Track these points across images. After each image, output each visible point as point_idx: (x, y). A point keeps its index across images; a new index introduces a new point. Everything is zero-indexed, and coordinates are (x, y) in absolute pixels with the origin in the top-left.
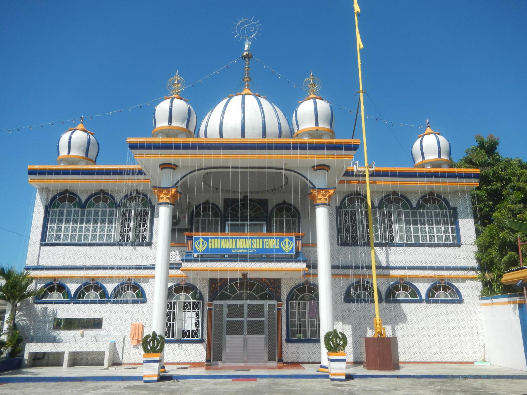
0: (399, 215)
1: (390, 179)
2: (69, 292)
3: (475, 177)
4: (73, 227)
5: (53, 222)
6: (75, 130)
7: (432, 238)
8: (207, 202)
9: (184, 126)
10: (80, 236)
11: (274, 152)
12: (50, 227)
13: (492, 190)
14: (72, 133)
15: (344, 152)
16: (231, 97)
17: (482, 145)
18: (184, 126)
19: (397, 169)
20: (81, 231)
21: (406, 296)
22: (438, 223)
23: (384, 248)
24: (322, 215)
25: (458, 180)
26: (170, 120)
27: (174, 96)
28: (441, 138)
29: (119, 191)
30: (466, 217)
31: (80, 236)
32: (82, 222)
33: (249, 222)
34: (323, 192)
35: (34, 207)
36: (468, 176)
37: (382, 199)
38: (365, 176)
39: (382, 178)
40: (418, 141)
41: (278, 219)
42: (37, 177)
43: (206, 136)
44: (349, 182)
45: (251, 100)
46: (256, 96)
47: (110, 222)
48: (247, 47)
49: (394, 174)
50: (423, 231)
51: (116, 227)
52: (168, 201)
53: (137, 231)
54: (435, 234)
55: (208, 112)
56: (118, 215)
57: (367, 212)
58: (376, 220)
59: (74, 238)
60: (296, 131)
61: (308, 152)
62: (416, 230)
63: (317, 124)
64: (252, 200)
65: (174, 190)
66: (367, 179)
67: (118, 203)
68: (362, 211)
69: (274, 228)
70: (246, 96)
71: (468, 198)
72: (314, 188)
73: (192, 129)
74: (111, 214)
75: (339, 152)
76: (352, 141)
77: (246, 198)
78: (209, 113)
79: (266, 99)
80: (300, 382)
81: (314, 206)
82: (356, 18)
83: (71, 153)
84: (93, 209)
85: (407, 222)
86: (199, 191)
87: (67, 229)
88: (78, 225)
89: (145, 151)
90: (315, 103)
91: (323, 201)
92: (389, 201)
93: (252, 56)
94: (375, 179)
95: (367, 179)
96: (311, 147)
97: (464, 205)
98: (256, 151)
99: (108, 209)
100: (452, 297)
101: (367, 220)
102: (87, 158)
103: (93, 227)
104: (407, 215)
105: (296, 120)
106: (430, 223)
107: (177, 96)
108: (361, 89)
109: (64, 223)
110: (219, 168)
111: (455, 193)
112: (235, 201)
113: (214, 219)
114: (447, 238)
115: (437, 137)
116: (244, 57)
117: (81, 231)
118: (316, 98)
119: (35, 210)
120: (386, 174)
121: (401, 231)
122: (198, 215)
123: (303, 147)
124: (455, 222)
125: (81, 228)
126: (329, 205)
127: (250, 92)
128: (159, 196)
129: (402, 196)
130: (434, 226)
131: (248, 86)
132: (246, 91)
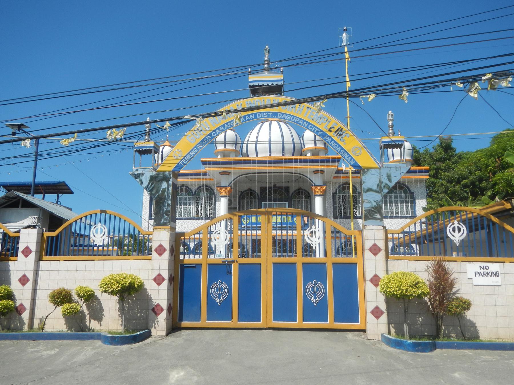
3: (425, 172)
6: (164, 146)
7: (397, 213)
8: (249, 189)
14: (163, 148)
15: (331, 163)
18: (233, 148)
22: (401, 202)
26: (225, 146)
30: (422, 198)
41: (296, 200)
44: (339, 177)
45: (275, 124)
47: (190, 204)
50: (391, 208)
51: (193, 207)
52: (226, 195)
53: (206, 209)
54: (399, 210)
56: (194, 201)
61: (308, 164)
65: (229, 188)
69: (293, 205)
70: (273, 122)
71: (424, 185)
72: (315, 185)
73: (238, 149)
74: (190, 200)
75: (328, 163)
77: (275, 186)
79: (285, 123)
86: (244, 182)
89: (212, 166)
91: (320, 193)
96: (310, 161)
97: (420, 190)
98: (277, 164)
100: (408, 251)
106: (396, 203)
110: (255, 173)
113: (254, 200)
114: (407, 212)
119: (144, 198)
122: (244, 198)
123: (306, 161)
124: (413, 202)
130: (399, 205)
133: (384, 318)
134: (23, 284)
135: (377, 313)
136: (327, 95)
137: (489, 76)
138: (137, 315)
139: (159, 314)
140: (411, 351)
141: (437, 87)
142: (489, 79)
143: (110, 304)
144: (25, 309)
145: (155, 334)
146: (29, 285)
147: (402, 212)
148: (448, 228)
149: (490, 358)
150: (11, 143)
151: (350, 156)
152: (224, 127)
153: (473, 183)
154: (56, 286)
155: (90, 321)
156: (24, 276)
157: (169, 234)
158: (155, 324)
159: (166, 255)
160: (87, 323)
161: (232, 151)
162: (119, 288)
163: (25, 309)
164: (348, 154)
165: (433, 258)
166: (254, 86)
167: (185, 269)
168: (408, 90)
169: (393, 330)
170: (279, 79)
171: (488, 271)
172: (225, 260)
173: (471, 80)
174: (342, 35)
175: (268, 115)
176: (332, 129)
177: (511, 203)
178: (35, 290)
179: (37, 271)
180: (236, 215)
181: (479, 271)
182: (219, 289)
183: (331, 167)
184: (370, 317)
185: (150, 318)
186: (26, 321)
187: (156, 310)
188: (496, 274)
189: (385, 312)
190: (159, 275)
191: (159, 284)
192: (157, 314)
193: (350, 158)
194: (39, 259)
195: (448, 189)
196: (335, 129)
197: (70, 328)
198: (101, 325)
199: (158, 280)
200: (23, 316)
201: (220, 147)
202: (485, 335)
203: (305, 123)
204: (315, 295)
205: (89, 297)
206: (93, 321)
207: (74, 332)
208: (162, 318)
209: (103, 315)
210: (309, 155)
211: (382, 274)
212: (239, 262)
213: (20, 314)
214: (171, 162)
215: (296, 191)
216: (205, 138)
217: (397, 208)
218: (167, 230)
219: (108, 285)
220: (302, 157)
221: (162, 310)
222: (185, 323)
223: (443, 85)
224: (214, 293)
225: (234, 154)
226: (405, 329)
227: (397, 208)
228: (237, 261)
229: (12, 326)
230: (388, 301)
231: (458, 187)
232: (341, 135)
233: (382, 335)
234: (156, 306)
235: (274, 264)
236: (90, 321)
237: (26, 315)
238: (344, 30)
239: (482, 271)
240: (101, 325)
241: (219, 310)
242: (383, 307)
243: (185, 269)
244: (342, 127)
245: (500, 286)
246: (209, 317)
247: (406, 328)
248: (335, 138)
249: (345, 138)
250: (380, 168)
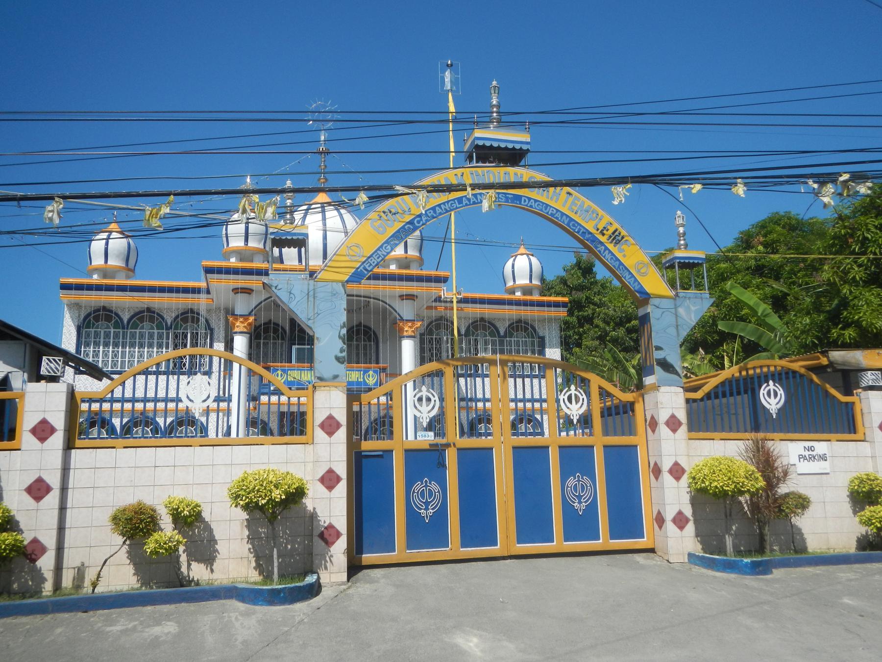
0: (486, 343)
1: (478, 306)
2: (113, 428)
4: (113, 352)
5: (87, 345)
6: (111, 232)
9: (261, 246)
10: (123, 363)
12: (85, 351)
13: (583, 317)
15: (433, 284)
17: (578, 264)
18: (261, 246)
19: (486, 296)
20: (123, 356)
24: (408, 349)
25: (546, 309)
26: (246, 240)
28: (534, 260)
29: (169, 309)
31: (123, 363)
32: (124, 346)
34: (410, 324)
35: (63, 326)
36: (557, 305)
37: (469, 326)
39: (470, 305)
40: (511, 260)
42: (73, 292)
44: (436, 308)
46: (337, 209)
49: (482, 301)
52: (245, 330)
57: (452, 339)
58: (461, 348)
59: (115, 365)
61: (397, 283)
63: (406, 251)
65: (251, 319)
66: (455, 305)
67: (169, 324)
68: (447, 339)
72: (402, 319)
75: (429, 284)
81: (402, 337)
83: (109, 263)
84: (138, 331)
87: (106, 355)
88: (120, 350)
89: (223, 276)
91: (410, 333)
92: (476, 328)
94: (463, 305)
95: (455, 305)
97: (552, 334)
99: (156, 331)
101: (452, 348)
102: (129, 269)
103: (139, 352)
104: (494, 344)
109: (101, 347)
111: (542, 320)
115: (529, 259)
117: (123, 356)
120: (474, 301)
123: (392, 277)
125: (124, 353)
129: (489, 322)
133: (690, 528)
134: (38, 498)
135: (680, 521)
136: (632, 177)
137: (845, 177)
138: (286, 546)
139: (333, 543)
140: (749, 574)
141: (781, 184)
142: (845, 182)
143: (230, 528)
144: (43, 550)
145: (328, 581)
146: (52, 500)
148: (762, 391)
149: (851, 575)
150: (15, 203)
151: (633, 276)
152: (435, 212)
154: (128, 499)
155: (189, 565)
156: (40, 481)
157: (345, 396)
158: (326, 561)
159: (341, 434)
160: (184, 569)
161: (257, 251)
162: (283, 497)
163: (43, 550)
164: (630, 273)
165: (753, 435)
166: (484, 146)
167: (364, 460)
168: (746, 184)
169: (700, 547)
170: (524, 139)
171: (814, 453)
172: (434, 442)
173: (821, 180)
174: (444, 72)
175: (507, 199)
176: (605, 232)
177: (828, 357)
178: (63, 509)
179: (66, 470)
180: (448, 365)
181: (803, 453)
182: (426, 494)
183: (434, 290)
184: (670, 527)
185: (315, 552)
186: (49, 575)
187: (326, 536)
188: (823, 458)
189: (691, 518)
190: (330, 471)
191: (330, 488)
192: (329, 543)
193: (633, 279)
194: (69, 446)
195: (607, 334)
196: (610, 232)
197: (145, 582)
198: (212, 571)
199: (329, 480)
200: (40, 563)
201: (237, 243)
202: (814, 544)
203: (564, 217)
204: (579, 497)
205: (189, 520)
206: (194, 565)
207: (155, 590)
208: (339, 549)
209: (217, 551)
210: (393, 268)
211: (683, 463)
212: (458, 446)
213: (34, 561)
214: (343, 264)
216: (403, 227)
218: (340, 388)
219: (258, 491)
220: (387, 271)
221: (338, 535)
222: (368, 558)
223: (787, 182)
224: (417, 501)
225: (261, 258)
226: (728, 543)
228: (454, 445)
229: (15, 586)
230: (694, 502)
231: (621, 332)
232: (616, 243)
233: (690, 555)
234: (326, 528)
235: (514, 448)
236: (189, 565)
237: (46, 563)
238: (448, 65)
239: (807, 453)
240: (212, 571)
241: (427, 531)
242: (688, 512)
243: (364, 460)
244: (620, 229)
245: (828, 474)
246: (412, 542)
247: (729, 541)
248: (610, 246)
249: (624, 247)
250: (675, 299)
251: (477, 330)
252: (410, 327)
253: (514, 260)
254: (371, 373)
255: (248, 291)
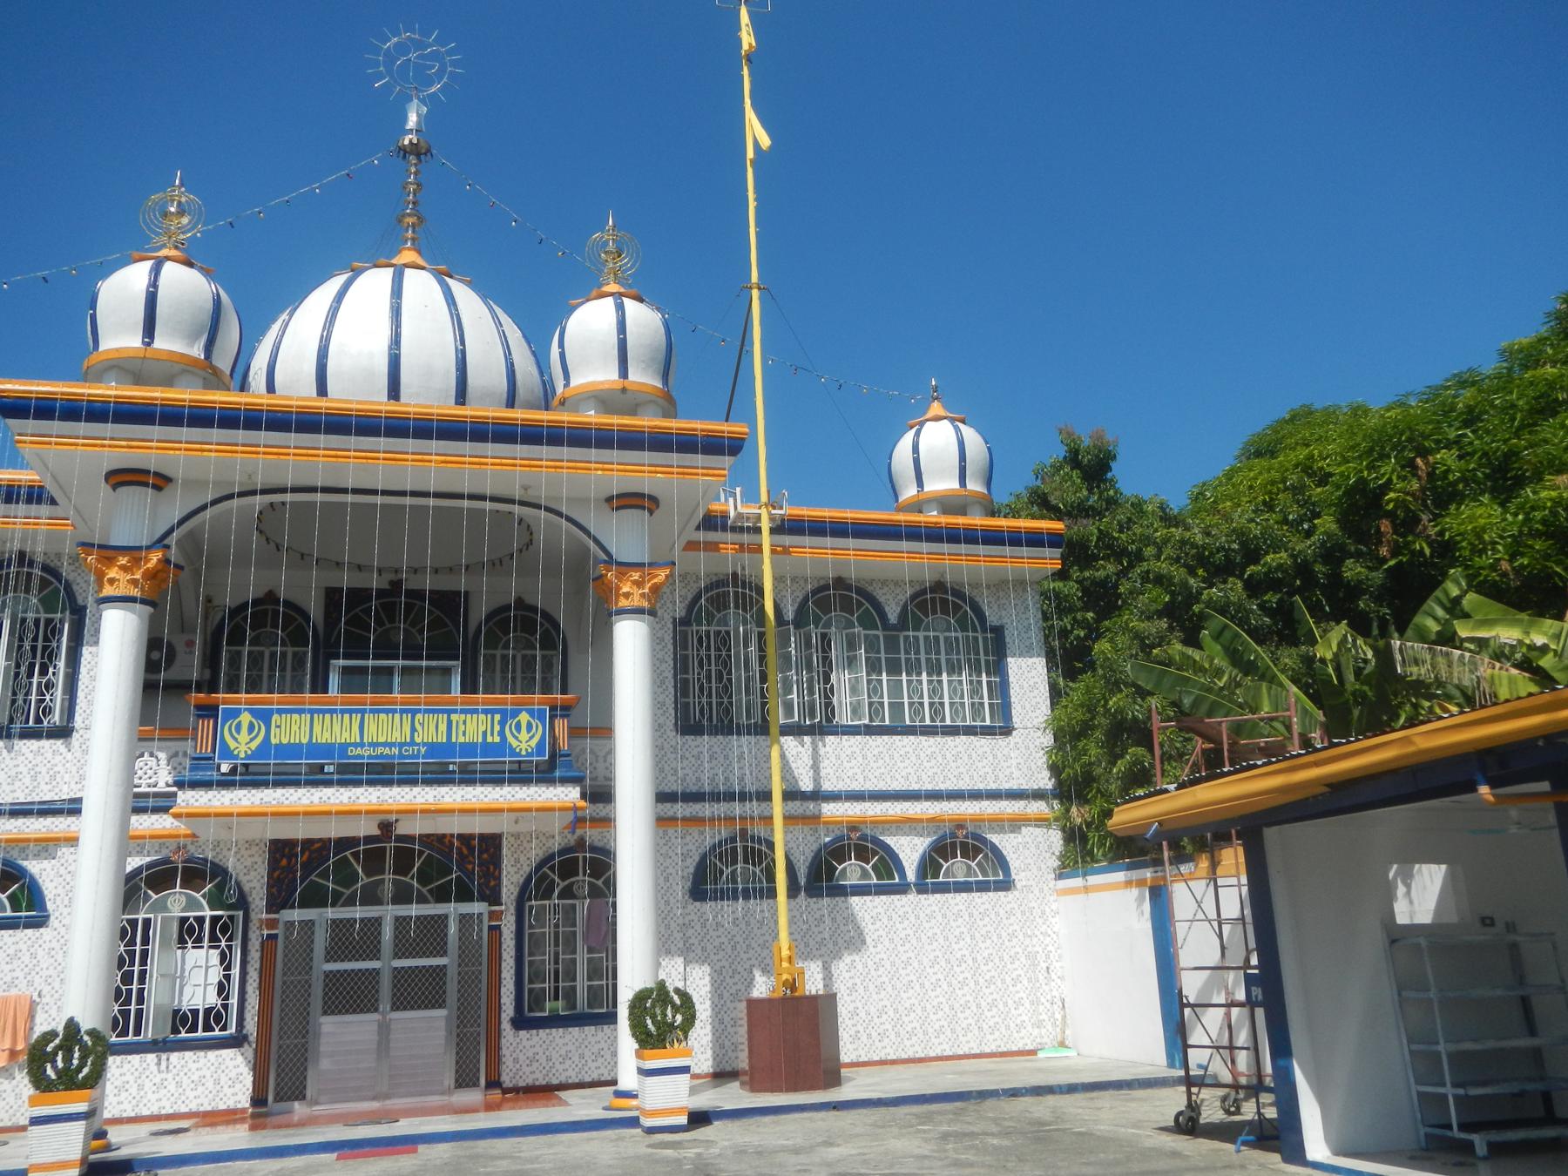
0: (852, 645)
1: (829, 541)
3: (1052, 545)
7: (937, 710)
8: (271, 597)
11: (490, 448)
13: (1095, 582)
15: (699, 459)
16: (357, 272)
17: (1073, 458)
18: (197, 351)
19: (849, 514)
21: (865, 874)
22: (954, 669)
23: (807, 739)
24: (632, 647)
25: (1007, 550)
27: (164, 252)
28: (969, 433)
30: (1027, 652)
33: (401, 662)
34: (636, 576)
36: (1035, 540)
37: (806, 599)
38: (758, 530)
39: (807, 540)
40: (908, 438)
41: (499, 653)
43: (271, 388)
44: (712, 547)
45: (421, 286)
46: (440, 275)
48: (412, 120)
49: (839, 529)
50: (915, 690)
54: (946, 700)
55: (282, 312)
57: (761, 635)
58: (787, 657)
60: (560, 389)
62: (896, 689)
63: (624, 372)
64: (416, 595)
65: (155, 558)
66: (766, 539)
73: (223, 362)
75: (688, 458)
76: (725, 428)
77: (396, 585)
78: (284, 316)
79: (469, 284)
80: (551, 1146)
82: (746, 72)
85: (873, 667)
86: (242, 560)
89: (56, 426)
90: (620, 308)
91: (636, 601)
93: (428, 151)
94: (787, 540)
95: (766, 539)
96: (603, 439)
97: (1022, 619)
98: (434, 445)
100: (984, 873)
101: (762, 659)
104: (872, 646)
105: (562, 356)
106: (935, 669)
107: (173, 253)
108: (755, 277)
111: (999, 586)
112: (359, 596)
113: (290, 650)
114: (977, 709)
115: (957, 430)
116: (404, 152)
118: (621, 295)
120: (818, 528)
121: (854, 690)
122: (237, 638)
123: (580, 437)
124: (998, 667)
126: (652, 613)
127: (421, 262)
128: (100, 576)
129: (860, 591)
130: (945, 677)
131: (413, 239)
132: (408, 256)
147: (956, 709)
153: (1303, 569)
195: (1193, 598)
215: (498, 616)
217: (935, 691)
227: (935, 691)
231: (1234, 589)
251: (827, 611)
252: (639, 584)
253: (918, 434)
254: (524, 717)
255: (160, 481)
